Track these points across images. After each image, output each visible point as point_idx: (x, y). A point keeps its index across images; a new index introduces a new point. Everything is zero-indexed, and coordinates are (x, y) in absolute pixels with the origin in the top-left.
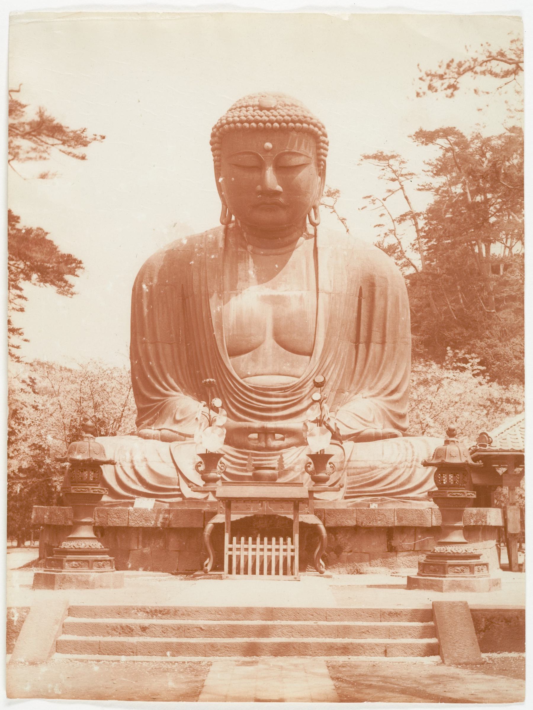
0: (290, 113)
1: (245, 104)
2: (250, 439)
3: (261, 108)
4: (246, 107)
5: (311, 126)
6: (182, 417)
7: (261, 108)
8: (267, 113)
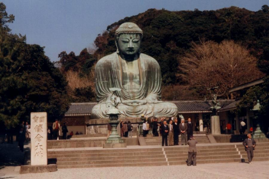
7: (129, 28)
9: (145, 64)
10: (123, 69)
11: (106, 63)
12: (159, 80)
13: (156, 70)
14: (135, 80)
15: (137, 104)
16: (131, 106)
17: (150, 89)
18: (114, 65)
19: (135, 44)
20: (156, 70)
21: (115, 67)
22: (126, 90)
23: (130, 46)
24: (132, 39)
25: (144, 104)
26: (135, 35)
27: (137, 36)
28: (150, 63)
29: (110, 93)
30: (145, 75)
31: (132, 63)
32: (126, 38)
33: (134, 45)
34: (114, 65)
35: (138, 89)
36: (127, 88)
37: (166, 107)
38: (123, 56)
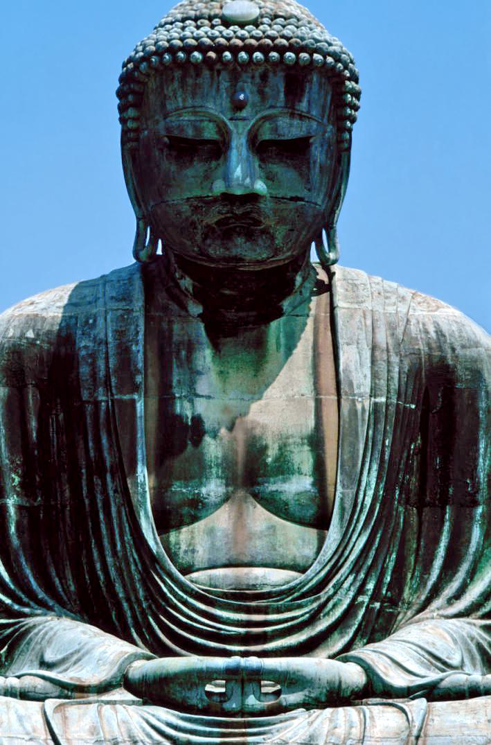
0: (286, 32)
1: (192, 13)
2: (209, 694)
3: (227, 22)
4: (196, 19)
5: (330, 60)
6: (59, 657)
7: (227, 22)
8: (241, 32)
9: (374, 348)
10: (175, 390)
11: (32, 343)
14: (272, 487)
16: (205, 711)
17: (423, 582)
18: (93, 356)
21: (102, 373)
22: (186, 570)
23: (226, 178)
25: (336, 697)
26: (278, 82)
28: (422, 347)
29: (51, 603)
30: (371, 443)
31: (260, 344)
32: (195, 113)
33: (270, 178)
34: (93, 356)
36: (201, 555)
38: (187, 283)
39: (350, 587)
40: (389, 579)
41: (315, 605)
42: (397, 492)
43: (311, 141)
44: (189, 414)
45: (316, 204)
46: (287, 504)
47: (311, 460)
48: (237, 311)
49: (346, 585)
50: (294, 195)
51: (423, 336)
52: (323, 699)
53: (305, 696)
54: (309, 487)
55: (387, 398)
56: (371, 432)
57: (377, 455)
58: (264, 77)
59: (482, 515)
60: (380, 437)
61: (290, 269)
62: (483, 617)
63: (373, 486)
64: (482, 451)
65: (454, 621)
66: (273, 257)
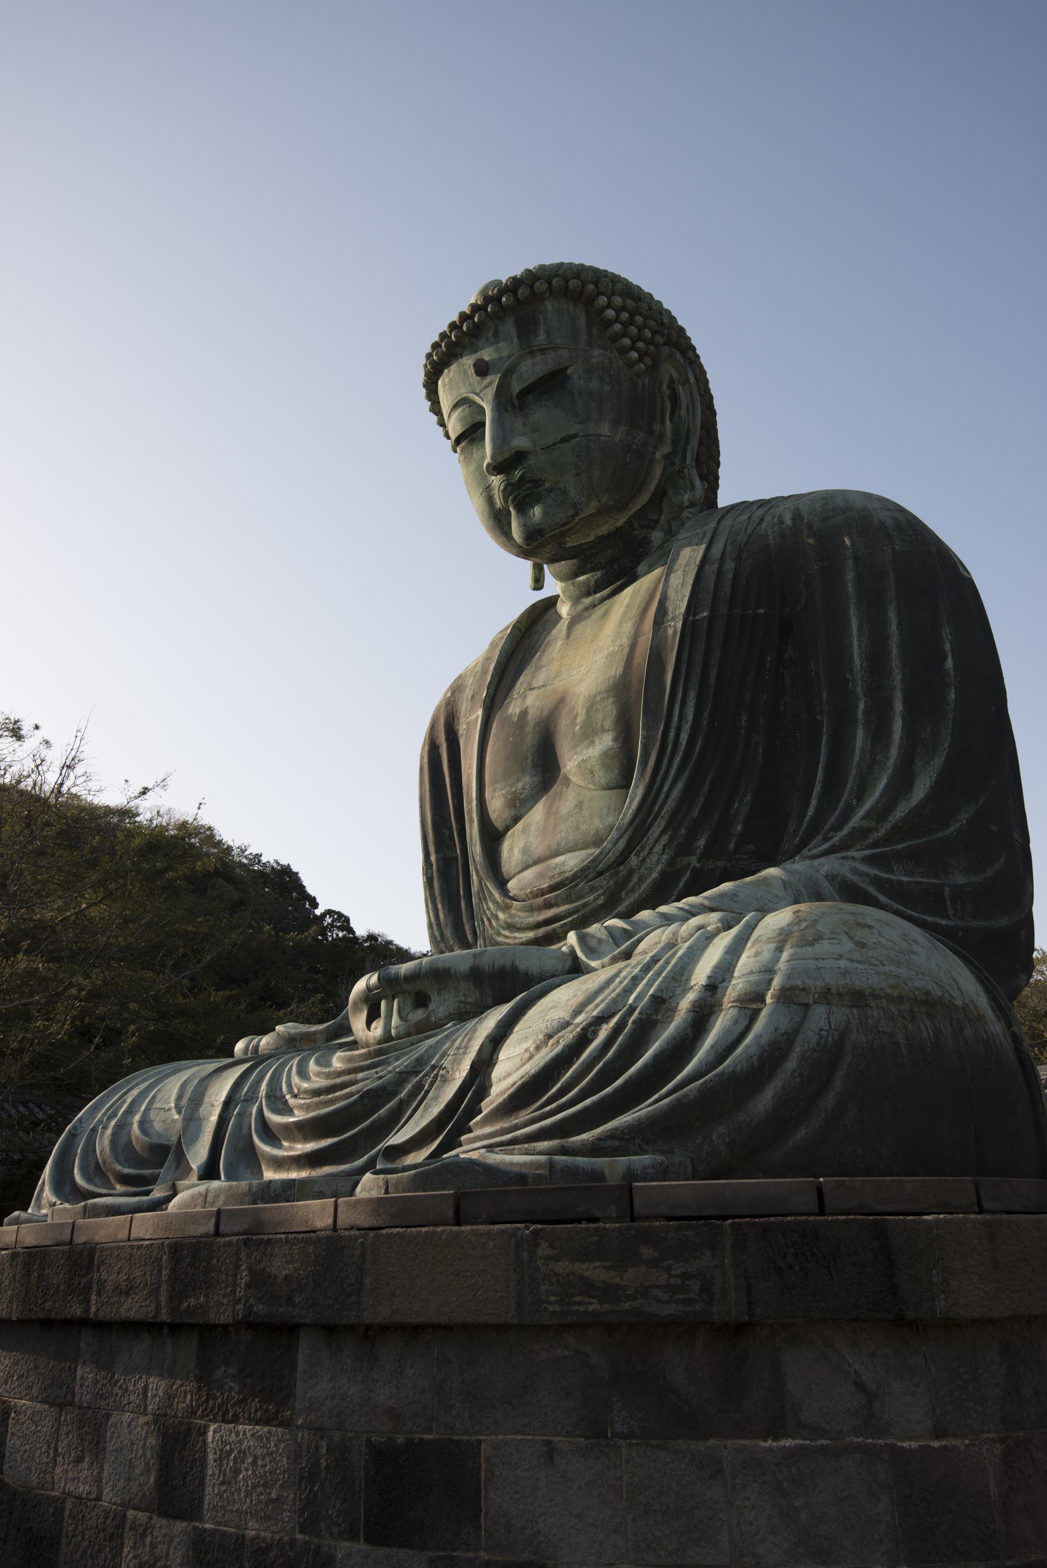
12: (897, 677)
13: (850, 576)
15: (419, 1015)
19: (539, 415)
20: (850, 576)
24: (494, 379)
26: (509, 327)
27: (526, 329)
31: (606, 614)
35: (597, 842)
37: (641, 996)
39: (663, 850)
40: (739, 828)
41: (611, 882)
42: (744, 718)
43: (569, 371)
44: (517, 711)
45: (600, 435)
46: (592, 772)
47: (615, 712)
48: (595, 593)
49: (658, 848)
50: (563, 435)
51: (776, 529)
52: (490, 1001)
53: (461, 1002)
54: (610, 743)
55: (713, 608)
56: (685, 656)
57: (695, 680)
58: (496, 334)
59: (866, 712)
60: (699, 658)
61: (636, 526)
62: (875, 845)
63: (690, 718)
64: (855, 631)
65: (823, 860)
66: (577, 514)
